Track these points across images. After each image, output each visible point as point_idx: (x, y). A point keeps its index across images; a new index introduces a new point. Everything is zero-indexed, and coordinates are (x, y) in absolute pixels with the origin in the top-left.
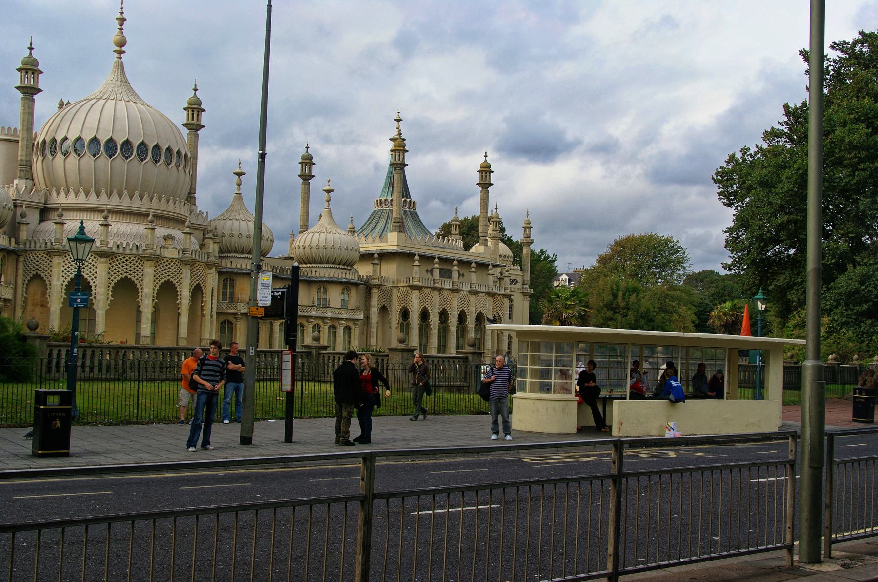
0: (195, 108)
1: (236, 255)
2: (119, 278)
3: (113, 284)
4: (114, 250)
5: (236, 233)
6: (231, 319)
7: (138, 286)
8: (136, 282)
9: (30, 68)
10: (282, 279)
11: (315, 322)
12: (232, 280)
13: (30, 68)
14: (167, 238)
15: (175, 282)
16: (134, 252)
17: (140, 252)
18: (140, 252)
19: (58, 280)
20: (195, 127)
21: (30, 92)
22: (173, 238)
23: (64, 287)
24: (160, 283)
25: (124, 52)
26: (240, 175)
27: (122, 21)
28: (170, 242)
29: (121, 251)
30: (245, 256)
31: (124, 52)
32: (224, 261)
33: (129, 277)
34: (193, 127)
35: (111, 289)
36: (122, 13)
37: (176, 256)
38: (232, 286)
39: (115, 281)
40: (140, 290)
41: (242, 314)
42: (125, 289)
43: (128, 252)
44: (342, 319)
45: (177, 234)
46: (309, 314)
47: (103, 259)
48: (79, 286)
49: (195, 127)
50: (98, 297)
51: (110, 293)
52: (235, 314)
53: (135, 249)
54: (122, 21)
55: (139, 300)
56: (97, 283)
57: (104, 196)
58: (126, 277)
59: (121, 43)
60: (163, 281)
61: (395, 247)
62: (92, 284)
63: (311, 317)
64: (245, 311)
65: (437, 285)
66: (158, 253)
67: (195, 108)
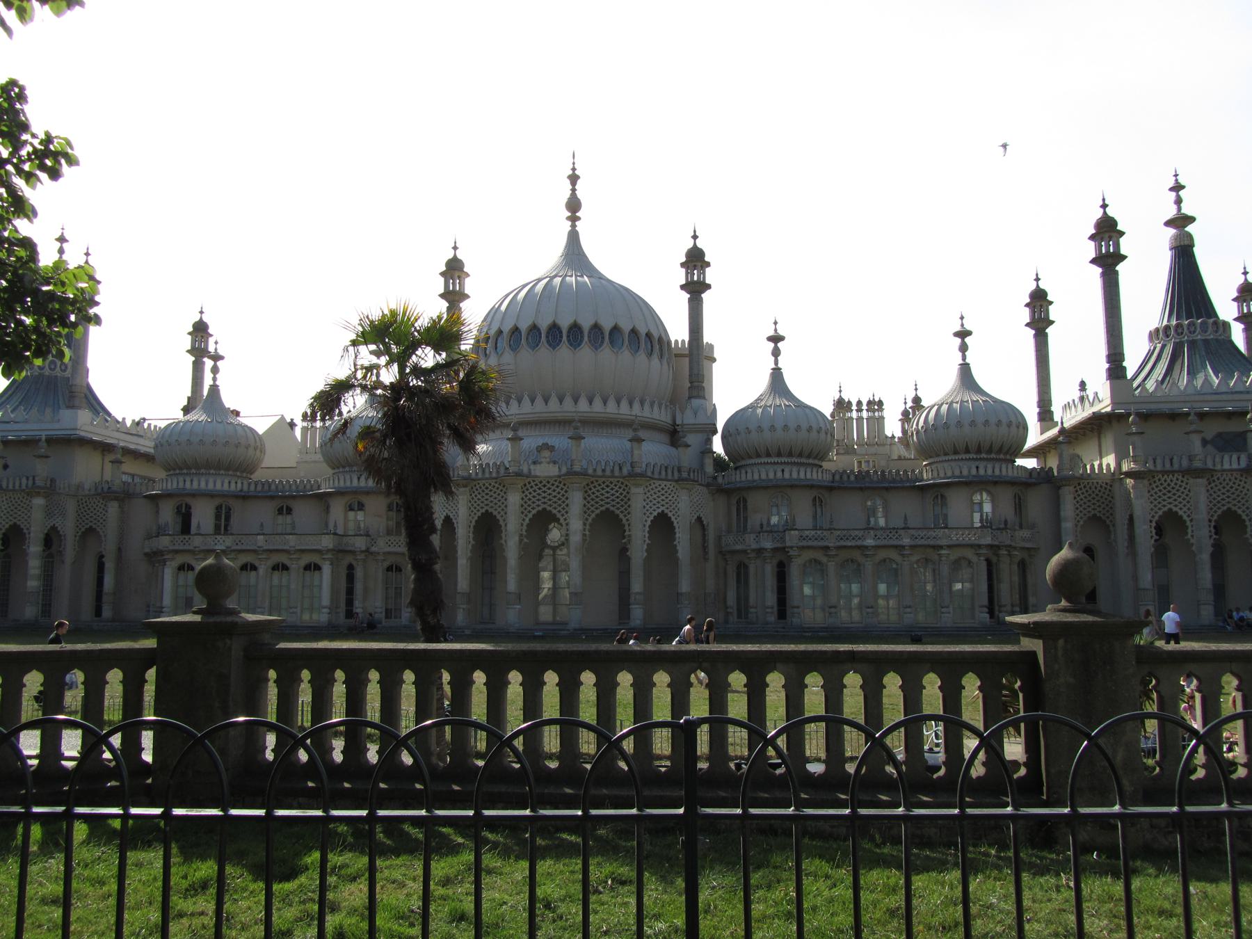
0: (695, 260)
1: (753, 461)
5: (804, 426)
7: (501, 523)
10: (861, 489)
11: (883, 554)
12: (745, 501)
14: (540, 449)
16: (494, 475)
20: (696, 289)
22: (551, 448)
24: (530, 516)
25: (579, 219)
27: (574, 179)
30: (763, 460)
31: (579, 219)
36: (574, 169)
38: (745, 508)
41: (753, 550)
43: (487, 475)
44: (941, 547)
45: (559, 440)
46: (859, 543)
49: (696, 289)
52: (745, 552)
54: (574, 179)
59: (574, 205)
60: (534, 512)
61: (1109, 409)
63: (866, 547)
64: (754, 546)
65: (1197, 464)
67: (695, 260)
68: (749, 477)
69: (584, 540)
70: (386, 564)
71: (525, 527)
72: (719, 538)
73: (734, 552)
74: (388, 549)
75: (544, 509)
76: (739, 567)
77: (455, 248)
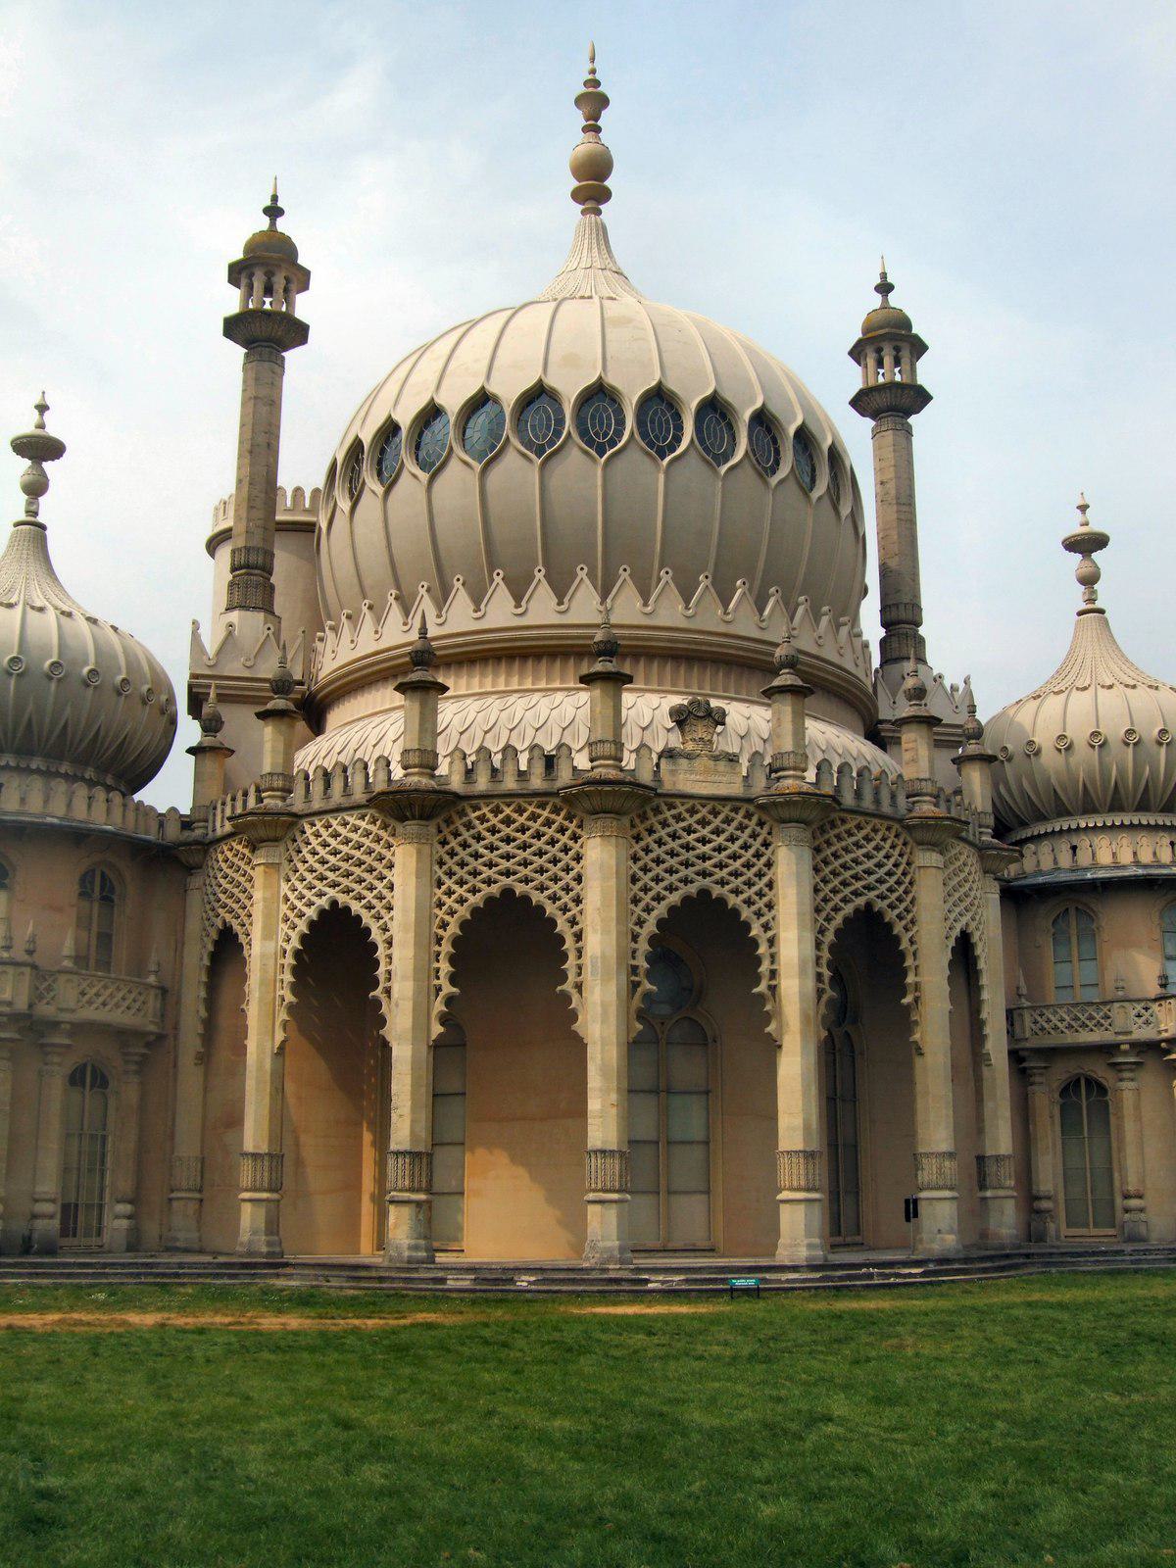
0: (890, 339)
2: (475, 900)
3: (453, 929)
4: (456, 784)
6: (1099, 1070)
7: (562, 925)
8: (550, 909)
9: (269, 265)
13: (269, 265)
15: (734, 901)
16: (537, 782)
17: (564, 776)
18: (564, 776)
19: (269, 934)
21: (266, 335)
23: (290, 960)
24: (660, 910)
26: (1087, 544)
28: (700, 731)
29: (482, 783)
32: (1045, 847)
33: (520, 889)
34: (880, 400)
35: (446, 948)
37: (735, 789)
39: (463, 912)
40: (569, 944)
42: (507, 950)
43: (510, 783)
47: (412, 827)
48: (337, 952)
50: (397, 988)
51: (445, 967)
52: (1108, 1050)
53: (539, 768)
55: (568, 987)
56: (395, 929)
57: (461, 600)
58: (508, 892)
60: (674, 898)
62: (376, 936)
66: (646, 777)
67: (890, 339)
68: (1083, 858)
69: (820, 992)
70: (70, 1063)
71: (643, 946)
72: (1010, 1014)
73: (1052, 1054)
74: (89, 1014)
75: (704, 893)
76: (1070, 1089)
77: (274, 211)
